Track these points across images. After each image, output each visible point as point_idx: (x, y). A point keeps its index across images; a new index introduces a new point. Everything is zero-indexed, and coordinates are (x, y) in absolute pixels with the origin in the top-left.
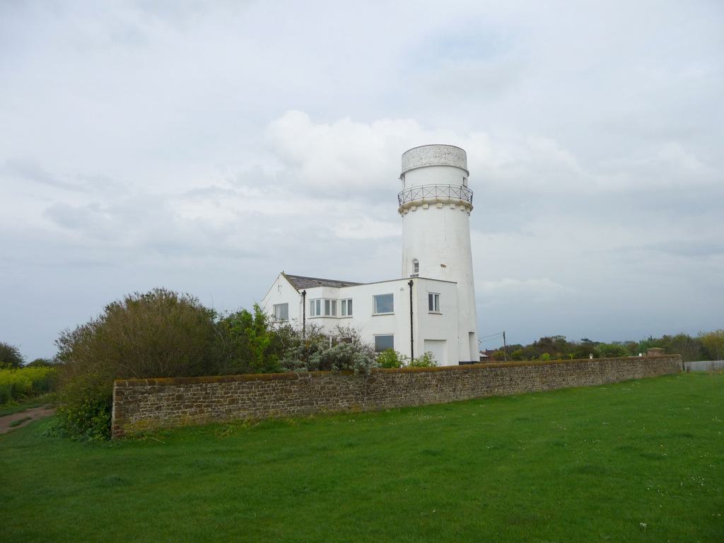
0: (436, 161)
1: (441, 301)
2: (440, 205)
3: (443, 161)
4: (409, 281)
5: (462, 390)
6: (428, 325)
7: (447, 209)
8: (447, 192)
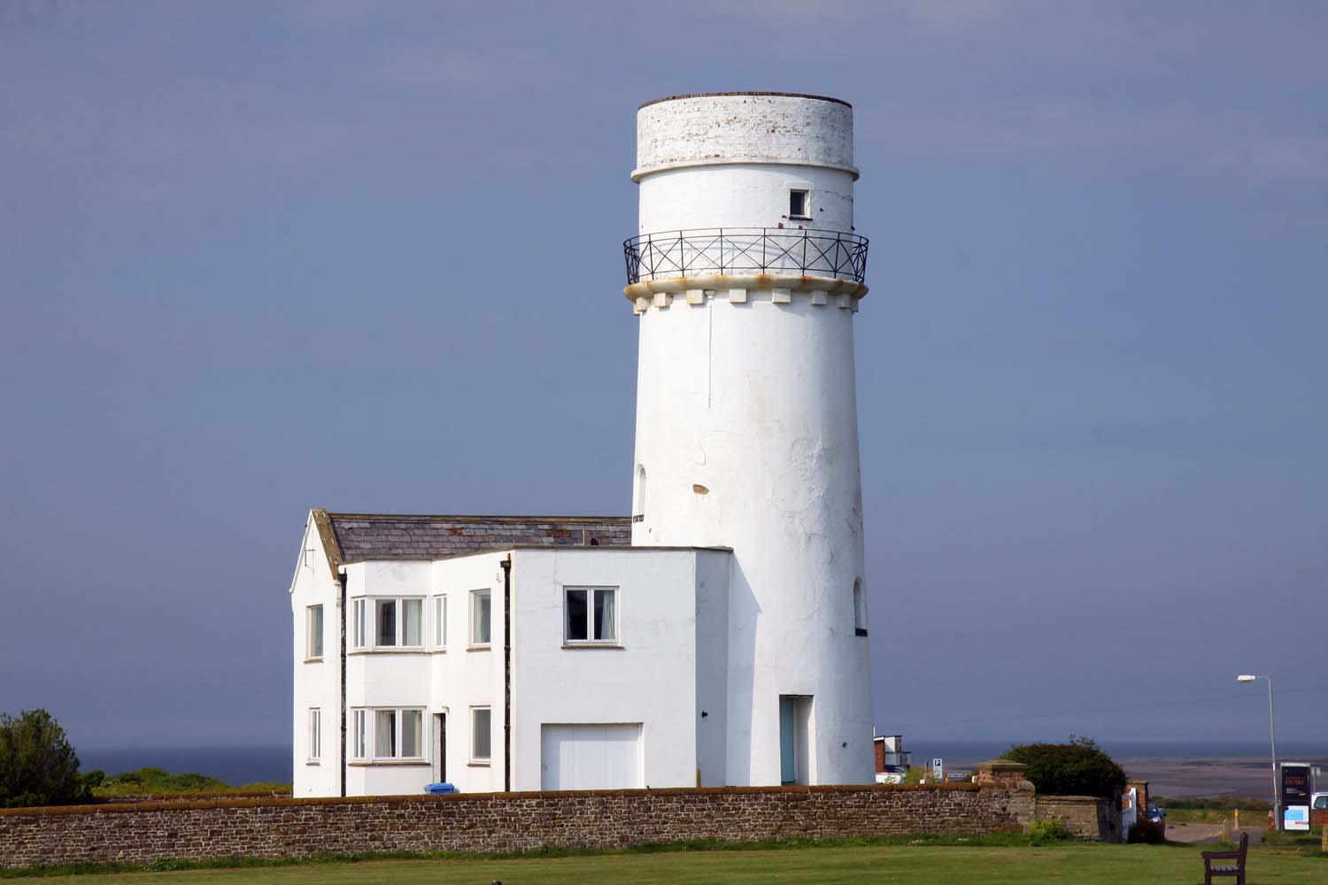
1: (621, 609)
2: (697, 295)
3: (710, 148)
4: (503, 556)
5: (14, 852)
7: (720, 304)
8: (714, 254)
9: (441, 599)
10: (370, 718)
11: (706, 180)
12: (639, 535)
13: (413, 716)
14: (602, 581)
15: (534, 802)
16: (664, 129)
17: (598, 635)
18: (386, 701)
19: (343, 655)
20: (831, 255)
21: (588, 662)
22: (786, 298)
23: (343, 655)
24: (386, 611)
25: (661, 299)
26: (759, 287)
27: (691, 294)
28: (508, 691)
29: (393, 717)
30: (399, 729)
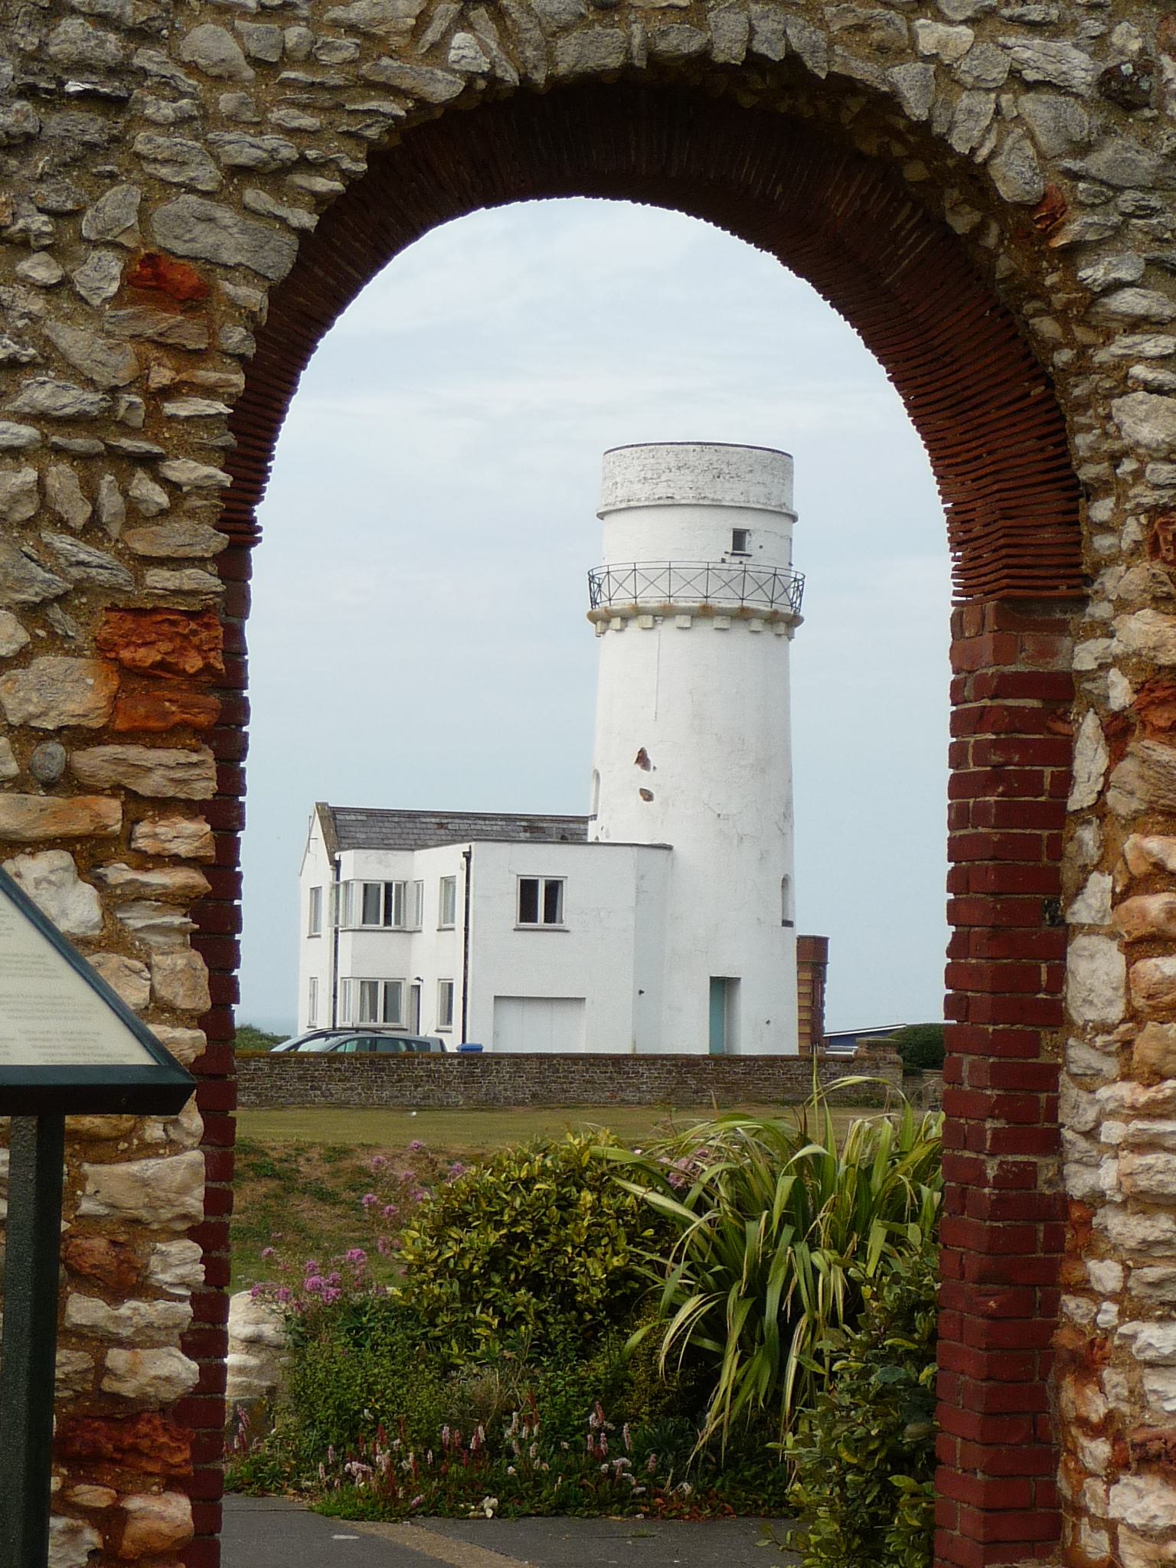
0: (643, 493)
3: (662, 491)
6: (537, 960)
8: (662, 583)
9: (419, 884)
10: (355, 989)
12: (593, 831)
13: (392, 989)
14: (553, 873)
15: (456, 1061)
17: (550, 917)
18: (369, 973)
19: (336, 932)
20: (768, 588)
21: (539, 943)
22: (725, 624)
23: (336, 932)
25: (616, 623)
26: (705, 613)
27: (643, 618)
28: (466, 967)
29: (374, 985)
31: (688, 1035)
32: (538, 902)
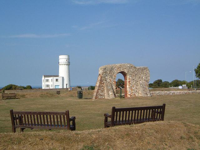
6: (57, 83)
11: (63, 59)
16: (61, 57)
24: (47, 80)
30: (48, 86)
31: (65, 87)
32: (57, 80)
